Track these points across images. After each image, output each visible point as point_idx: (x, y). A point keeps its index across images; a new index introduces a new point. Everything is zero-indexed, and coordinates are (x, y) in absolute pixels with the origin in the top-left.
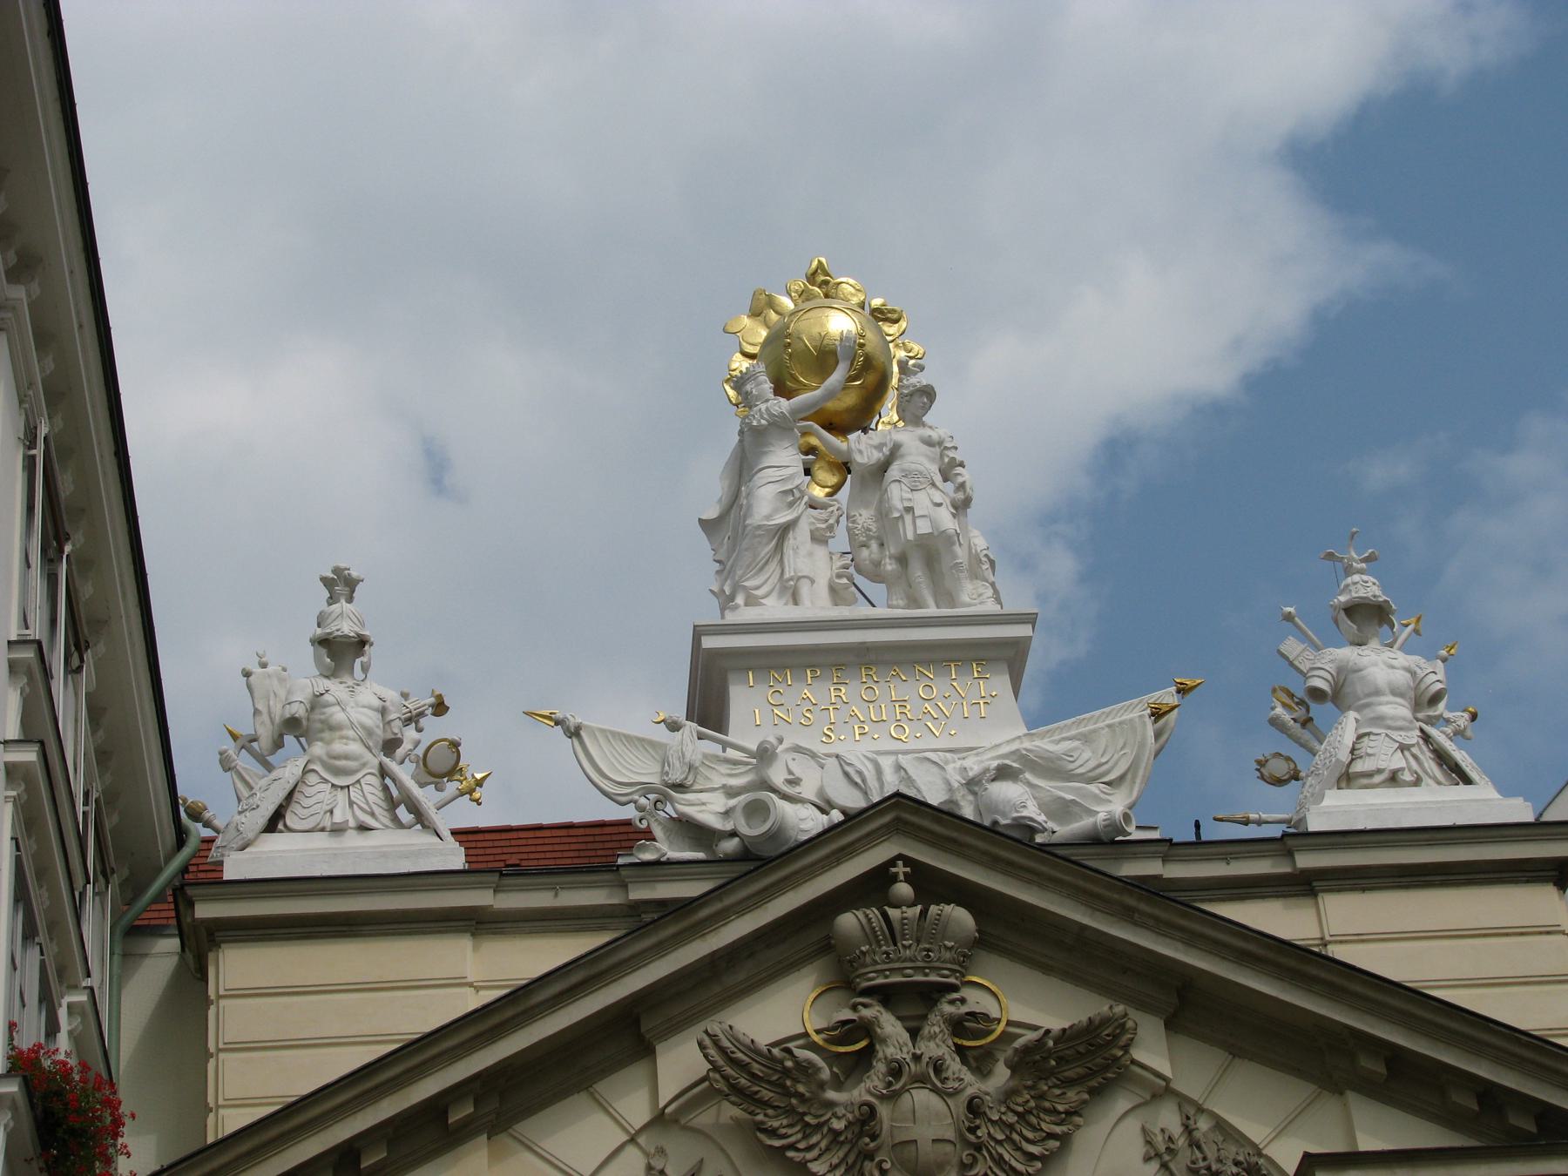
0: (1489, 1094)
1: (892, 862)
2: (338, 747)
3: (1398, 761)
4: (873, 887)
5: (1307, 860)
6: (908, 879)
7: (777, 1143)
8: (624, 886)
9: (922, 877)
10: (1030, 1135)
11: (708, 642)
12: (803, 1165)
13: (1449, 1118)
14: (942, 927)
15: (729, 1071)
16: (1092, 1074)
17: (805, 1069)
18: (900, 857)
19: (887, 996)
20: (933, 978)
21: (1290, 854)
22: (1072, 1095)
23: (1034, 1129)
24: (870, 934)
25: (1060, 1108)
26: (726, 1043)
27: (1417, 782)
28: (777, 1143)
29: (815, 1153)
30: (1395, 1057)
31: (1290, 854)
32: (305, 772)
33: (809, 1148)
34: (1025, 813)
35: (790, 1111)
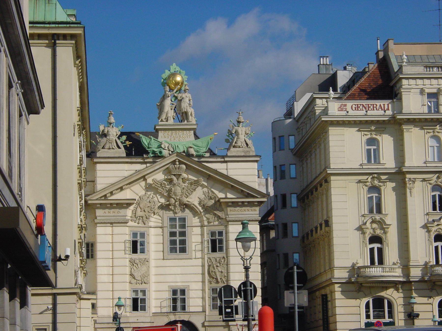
0: (242, 191)
1: (176, 159)
2: (111, 138)
3: (240, 145)
4: (174, 162)
5: (226, 159)
6: (178, 162)
7: (161, 191)
8: (144, 159)
9: (180, 161)
10: (190, 191)
11: (157, 127)
12: (163, 194)
13: (238, 192)
14: (182, 168)
15: (155, 184)
16: (198, 185)
17: (164, 184)
18: (177, 159)
19: (174, 175)
20: (180, 173)
21: (224, 158)
22: (195, 187)
23: (190, 191)
24: (173, 169)
25: (194, 189)
26: (155, 181)
27: (242, 147)
28: (161, 191)
29: (164, 193)
30: (232, 186)
31: (224, 158)
32: (107, 140)
33: (164, 192)
34: (192, 153)
35: (162, 188)
